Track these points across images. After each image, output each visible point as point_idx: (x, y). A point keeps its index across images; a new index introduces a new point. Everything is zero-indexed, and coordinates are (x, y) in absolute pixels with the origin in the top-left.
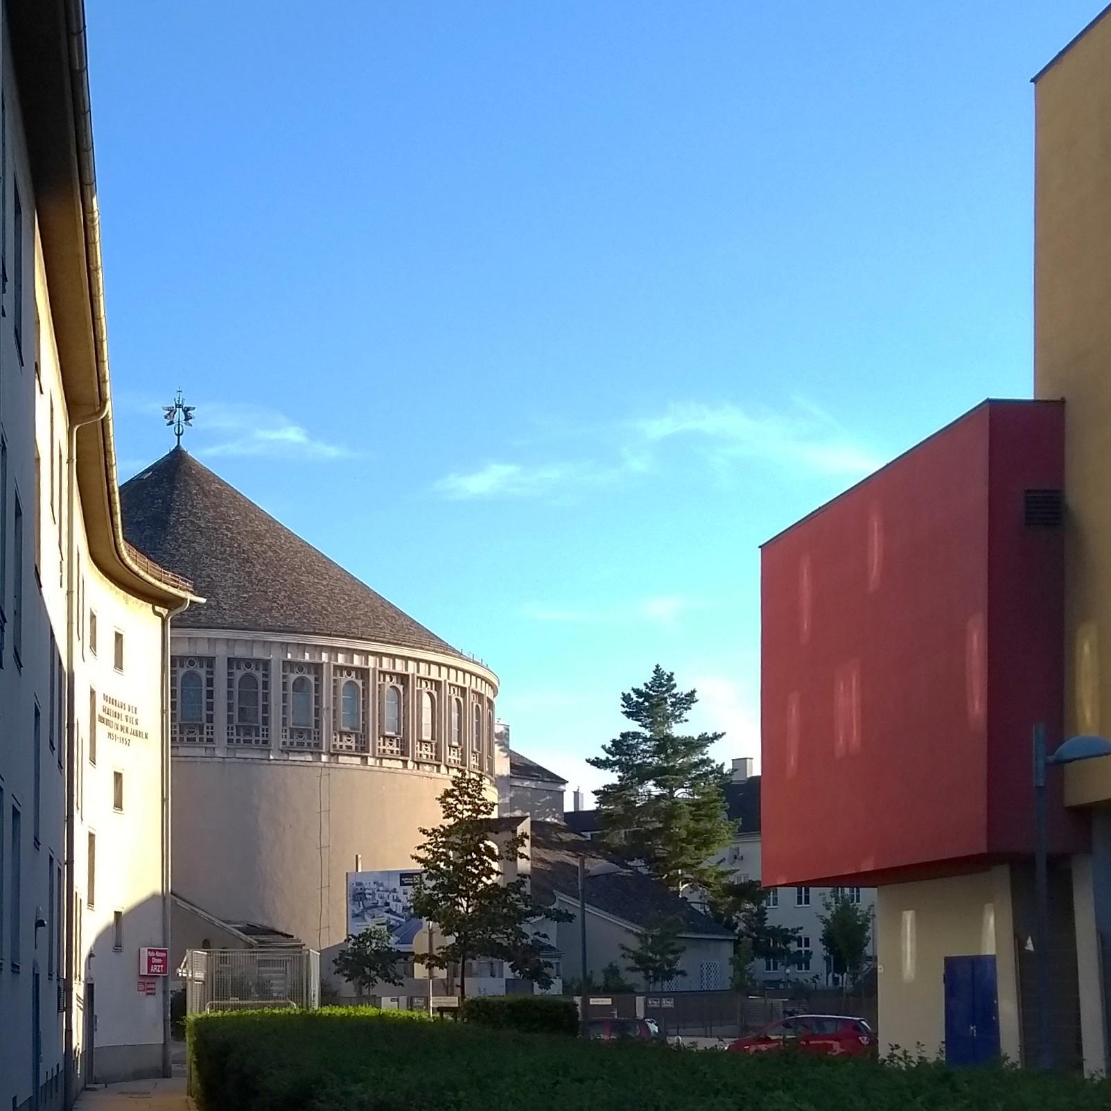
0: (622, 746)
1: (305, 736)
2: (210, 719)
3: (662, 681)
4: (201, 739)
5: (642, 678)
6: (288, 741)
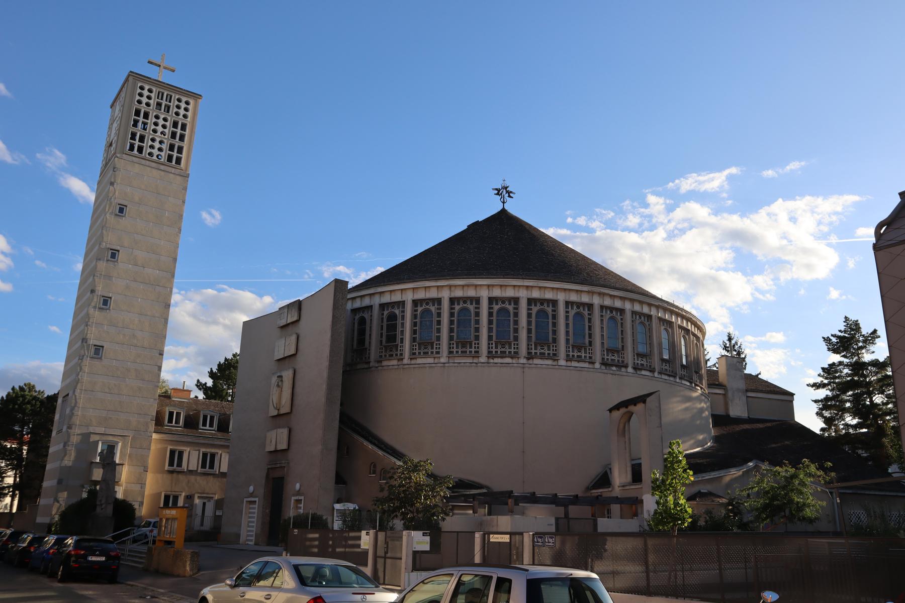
0: (830, 370)
1: (507, 347)
2: (438, 338)
3: (853, 327)
4: (432, 353)
5: (837, 327)
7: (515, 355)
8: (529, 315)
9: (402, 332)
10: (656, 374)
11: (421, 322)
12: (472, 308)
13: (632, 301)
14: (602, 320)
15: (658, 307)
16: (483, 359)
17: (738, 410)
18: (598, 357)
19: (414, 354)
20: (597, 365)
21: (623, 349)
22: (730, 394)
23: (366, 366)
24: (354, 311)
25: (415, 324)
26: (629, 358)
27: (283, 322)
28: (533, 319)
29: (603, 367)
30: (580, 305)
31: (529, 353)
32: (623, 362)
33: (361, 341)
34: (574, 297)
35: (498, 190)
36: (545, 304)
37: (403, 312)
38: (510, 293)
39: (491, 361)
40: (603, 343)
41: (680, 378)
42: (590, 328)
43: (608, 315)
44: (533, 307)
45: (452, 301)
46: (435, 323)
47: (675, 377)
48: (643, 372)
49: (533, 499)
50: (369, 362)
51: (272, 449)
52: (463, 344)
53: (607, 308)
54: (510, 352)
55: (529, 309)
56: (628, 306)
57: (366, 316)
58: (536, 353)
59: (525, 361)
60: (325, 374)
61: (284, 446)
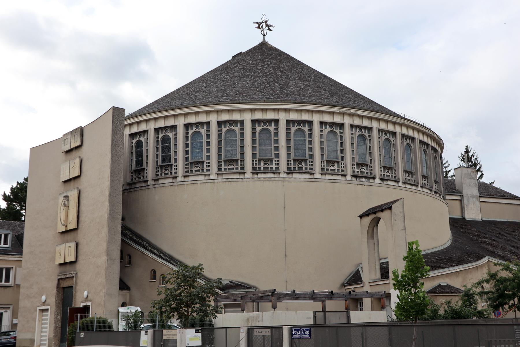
1: (269, 163)
2: (208, 157)
6: (257, 166)
8: (288, 135)
9: (176, 152)
10: (400, 184)
11: (192, 144)
13: (379, 120)
14: (352, 137)
15: (401, 125)
16: (248, 175)
17: (473, 213)
18: (349, 171)
19: (187, 172)
20: (349, 178)
21: (371, 163)
22: (465, 201)
23: (143, 184)
24: (132, 136)
25: (187, 145)
26: (377, 170)
27: (67, 148)
29: (354, 179)
30: (332, 124)
31: (288, 168)
32: (371, 174)
33: (139, 162)
34: (327, 118)
35: (259, 24)
36: (302, 125)
37: (176, 135)
38: (271, 116)
39: (256, 176)
40: (353, 158)
41: (422, 187)
42: (342, 144)
43: (357, 133)
44: (291, 127)
46: (204, 144)
47: (417, 186)
48: (389, 183)
49: (294, 296)
50: (147, 181)
51: (62, 261)
52: (230, 163)
53: (357, 127)
54: (272, 168)
55: (287, 129)
56: (375, 125)
57: (143, 139)
58: (295, 168)
59: (285, 175)
60: (107, 193)
61: (71, 258)
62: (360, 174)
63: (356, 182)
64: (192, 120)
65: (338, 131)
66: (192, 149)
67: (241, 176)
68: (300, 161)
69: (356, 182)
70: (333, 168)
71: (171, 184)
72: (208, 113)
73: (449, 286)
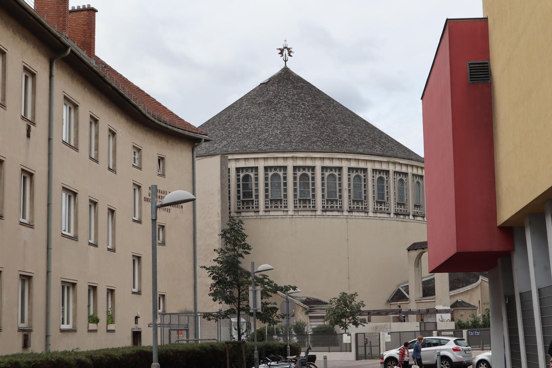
1: (334, 203)
2: (286, 196)
6: (326, 205)
7: (341, 210)
12: (310, 174)
16: (319, 213)
18: (371, 208)
20: (392, 215)
26: (411, 209)
28: (352, 182)
29: (395, 217)
36: (359, 171)
38: (336, 164)
39: (324, 214)
40: (374, 197)
45: (295, 168)
52: (305, 201)
58: (354, 207)
62: (399, 212)
63: (398, 219)
64: (271, 163)
65: (385, 177)
66: (271, 189)
67: (313, 213)
68: (358, 202)
69: (398, 219)
70: (381, 207)
71: (255, 217)
72: (285, 158)
73: (463, 302)
